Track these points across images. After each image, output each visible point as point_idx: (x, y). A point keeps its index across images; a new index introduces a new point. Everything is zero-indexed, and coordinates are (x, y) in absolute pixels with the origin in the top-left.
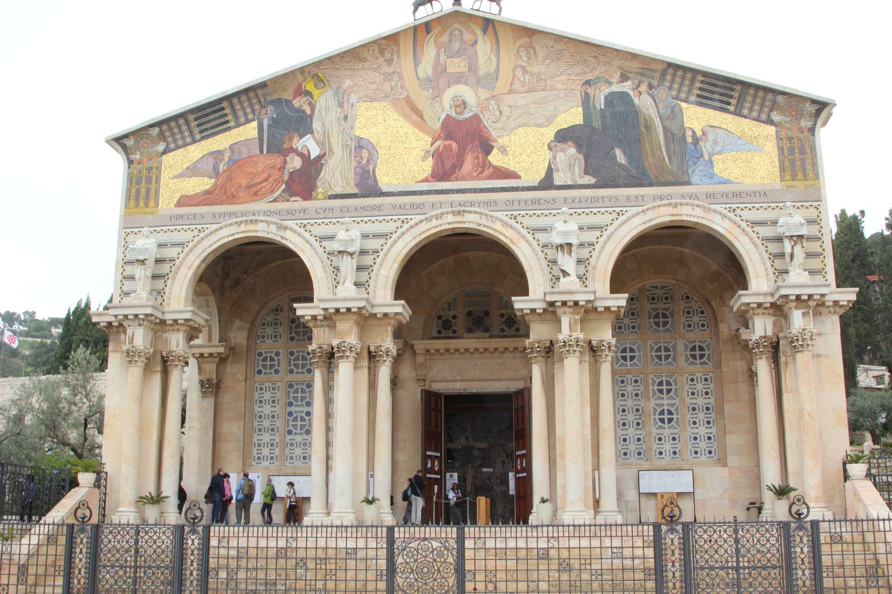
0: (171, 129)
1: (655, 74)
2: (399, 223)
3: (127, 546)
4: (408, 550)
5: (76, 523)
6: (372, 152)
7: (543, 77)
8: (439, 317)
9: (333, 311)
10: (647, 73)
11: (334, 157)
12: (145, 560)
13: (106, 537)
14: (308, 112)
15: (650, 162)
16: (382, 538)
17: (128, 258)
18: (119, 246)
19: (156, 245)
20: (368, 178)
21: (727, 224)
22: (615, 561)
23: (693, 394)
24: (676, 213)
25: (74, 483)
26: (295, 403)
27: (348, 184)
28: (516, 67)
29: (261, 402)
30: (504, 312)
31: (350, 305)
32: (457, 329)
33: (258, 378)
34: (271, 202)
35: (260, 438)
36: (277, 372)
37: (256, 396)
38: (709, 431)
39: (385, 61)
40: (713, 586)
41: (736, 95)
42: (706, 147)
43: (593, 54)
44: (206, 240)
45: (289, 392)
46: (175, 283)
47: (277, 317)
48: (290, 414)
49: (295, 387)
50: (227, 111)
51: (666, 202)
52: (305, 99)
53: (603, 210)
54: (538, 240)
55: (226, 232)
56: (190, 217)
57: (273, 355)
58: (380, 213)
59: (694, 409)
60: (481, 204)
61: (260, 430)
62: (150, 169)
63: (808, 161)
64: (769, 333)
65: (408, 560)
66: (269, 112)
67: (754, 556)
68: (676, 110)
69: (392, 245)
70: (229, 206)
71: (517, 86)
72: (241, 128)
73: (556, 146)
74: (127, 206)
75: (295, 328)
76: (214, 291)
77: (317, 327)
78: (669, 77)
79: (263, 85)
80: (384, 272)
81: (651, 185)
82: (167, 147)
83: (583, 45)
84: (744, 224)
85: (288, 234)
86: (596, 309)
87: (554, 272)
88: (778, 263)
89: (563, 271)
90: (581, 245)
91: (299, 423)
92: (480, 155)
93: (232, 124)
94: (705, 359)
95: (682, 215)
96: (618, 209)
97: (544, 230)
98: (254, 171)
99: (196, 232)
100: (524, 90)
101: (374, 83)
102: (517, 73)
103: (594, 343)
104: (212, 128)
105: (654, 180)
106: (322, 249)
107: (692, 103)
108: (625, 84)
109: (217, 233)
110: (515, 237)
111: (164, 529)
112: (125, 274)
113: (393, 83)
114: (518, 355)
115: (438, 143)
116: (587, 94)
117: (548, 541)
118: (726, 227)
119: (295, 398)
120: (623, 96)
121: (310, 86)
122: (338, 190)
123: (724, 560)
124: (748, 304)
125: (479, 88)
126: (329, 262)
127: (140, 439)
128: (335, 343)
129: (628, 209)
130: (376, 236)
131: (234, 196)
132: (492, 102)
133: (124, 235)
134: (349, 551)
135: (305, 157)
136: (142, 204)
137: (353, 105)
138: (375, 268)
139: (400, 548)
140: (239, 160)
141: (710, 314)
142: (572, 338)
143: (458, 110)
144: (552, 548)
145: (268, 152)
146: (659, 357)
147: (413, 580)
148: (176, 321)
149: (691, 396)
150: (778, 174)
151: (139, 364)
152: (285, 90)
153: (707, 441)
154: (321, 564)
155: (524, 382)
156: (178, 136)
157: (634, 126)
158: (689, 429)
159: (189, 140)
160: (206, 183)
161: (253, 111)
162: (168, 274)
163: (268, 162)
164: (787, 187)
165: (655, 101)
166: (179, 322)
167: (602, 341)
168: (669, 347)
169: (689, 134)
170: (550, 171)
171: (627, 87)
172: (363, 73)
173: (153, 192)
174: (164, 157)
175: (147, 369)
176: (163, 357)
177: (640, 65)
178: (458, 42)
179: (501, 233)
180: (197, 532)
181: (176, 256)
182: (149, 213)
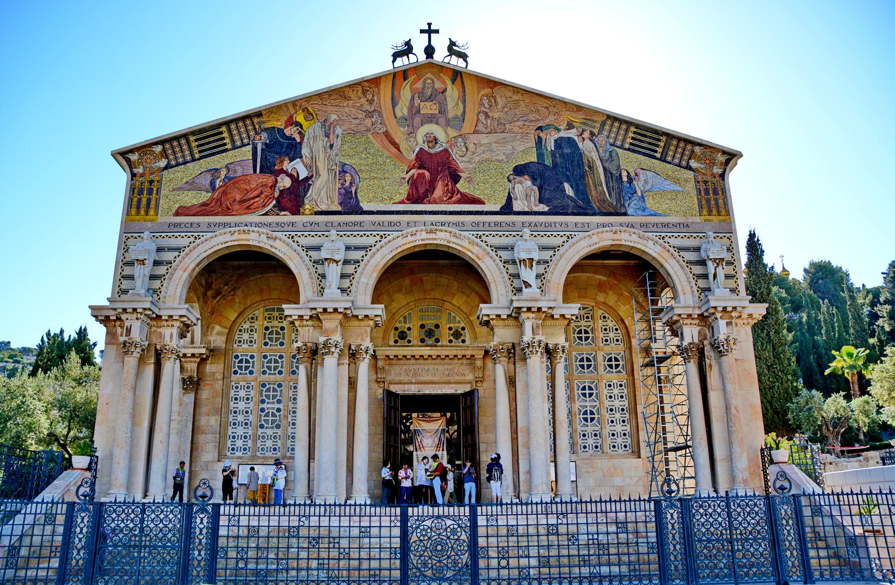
0: (173, 148)
1: (596, 124)
2: (378, 238)
3: (131, 525)
4: (422, 527)
5: (78, 501)
6: (354, 176)
7: (502, 121)
8: (396, 329)
9: (321, 310)
10: (590, 123)
11: (320, 179)
12: (151, 539)
13: (109, 516)
14: (298, 140)
15: (593, 194)
16: (396, 516)
17: (127, 259)
18: (119, 248)
19: (155, 248)
20: (351, 198)
21: (658, 249)
22: (620, 535)
23: (611, 397)
24: (616, 238)
25: (69, 465)
26: (267, 400)
27: (332, 202)
28: (480, 113)
29: (236, 399)
30: (452, 325)
31: (336, 305)
32: (411, 339)
33: (234, 377)
34: (262, 215)
35: (234, 430)
36: (251, 373)
37: (232, 394)
38: (624, 428)
39: (367, 101)
40: (711, 557)
41: (662, 144)
42: (639, 185)
43: (545, 105)
44: (201, 245)
45: (262, 391)
46: (171, 284)
47: (253, 325)
48: (262, 410)
49: (268, 387)
50: (226, 135)
51: (608, 228)
52: (295, 129)
53: (555, 233)
54: (500, 257)
55: (221, 239)
56: (187, 226)
57: (248, 358)
58: (361, 229)
59: (611, 410)
60: (451, 224)
61: (234, 424)
62: (151, 182)
63: (721, 201)
64: (696, 340)
65: (422, 538)
66: (262, 138)
67: (745, 528)
68: (613, 154)
69: (371, 257)
70: (223, 217)
71: (480, 127)
72: (237, 150)
73: (514, 179)
74: (128, 214)
75: (269, 334)
76: (198, 300)
77: (303, 326)
78: (607, 127)
79: (259, 114)
80: (363, 280)
81: (594, 214)
82: (168, 163)
83: (537, 97)
84: (672, 250)
85: (277, 243)
86: (552, 316)
87: (514, 285)
88: (702, 283)
89: (525, 282)
90: (539, 262)
91: (270, 418)
92: (450, 183)
93: (229, 146)
94: (619, 368)
95: (621, 240)
96: (568, 234)
97: (505, 248)
98: (248, 188)
99: (192, 239)
100: (486, 131)
101: (357, 118)
102: (480, 117)
103: (550, 346)
104: (210, 149)
105: (597, 211)
106: (308, 258)
107: (625, 149)
108: (570, 131)
109: (212, 240)
110: (481, 253)
111: (172, 508)
112: (124, 273)
113: (373, 120)
114: (465, 361)
115: (413, 171)
116: (539, 137)
117: (558, 517)
118: (657, 251)
119: (268, 397)
120: (570, 141)
121: (300, 118)
122: (324, 207)
123: (719, 533)
124: (680, 315)
125: (448, 128)
126: (314, 269)
127: (133, 425)
128: (322, 339)
129: (576, 233)
130: (357, 248)
131: (229, 209)
132: (460, 140)
133: (124, 239)
134: (363, 529)
135: (294, 179)
136: (142, 213)
137: (338, 136)
138: (356, 276)
139: (414, 526)
140: (233, 178)
141: (624, 331)
142: (535, 340)
143: (430, 145)
144: (561, 524)
145: (260, 173)
146: (582, 367)
147: (427, 558)
148: (171, 317)
149: (609, 399)
150: (698, 210)
151: (135, 354)
152: (278, 120)
153: (623, 437)
154: (334, 543)
155: (469, 385)
156: (179, 155)
157: (579, 166)
158: (608, 427)
159: (188, 158)
160: (205, 197)
161: (249, 137)
162: (164, 275)
163: (261, 180)
164: (705, 221)
165: (596, 146)
166: (174, 318)
167: (556, 345)
168: (590, 358)
169: (624, 174)
170: (509, 199)
171: (573, 134)
172: (347, 110)
173: (153, 202)
174: (165, 172)
175: (142, 360)
176: (156, 350)
177: (583, 117)
178: (430, 90)
179: (469, 250)
180: (207, 512)
181: (173, 260)
182: (149, 221)
